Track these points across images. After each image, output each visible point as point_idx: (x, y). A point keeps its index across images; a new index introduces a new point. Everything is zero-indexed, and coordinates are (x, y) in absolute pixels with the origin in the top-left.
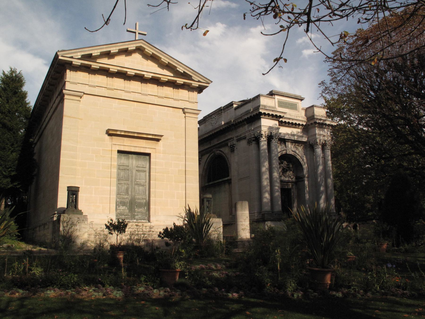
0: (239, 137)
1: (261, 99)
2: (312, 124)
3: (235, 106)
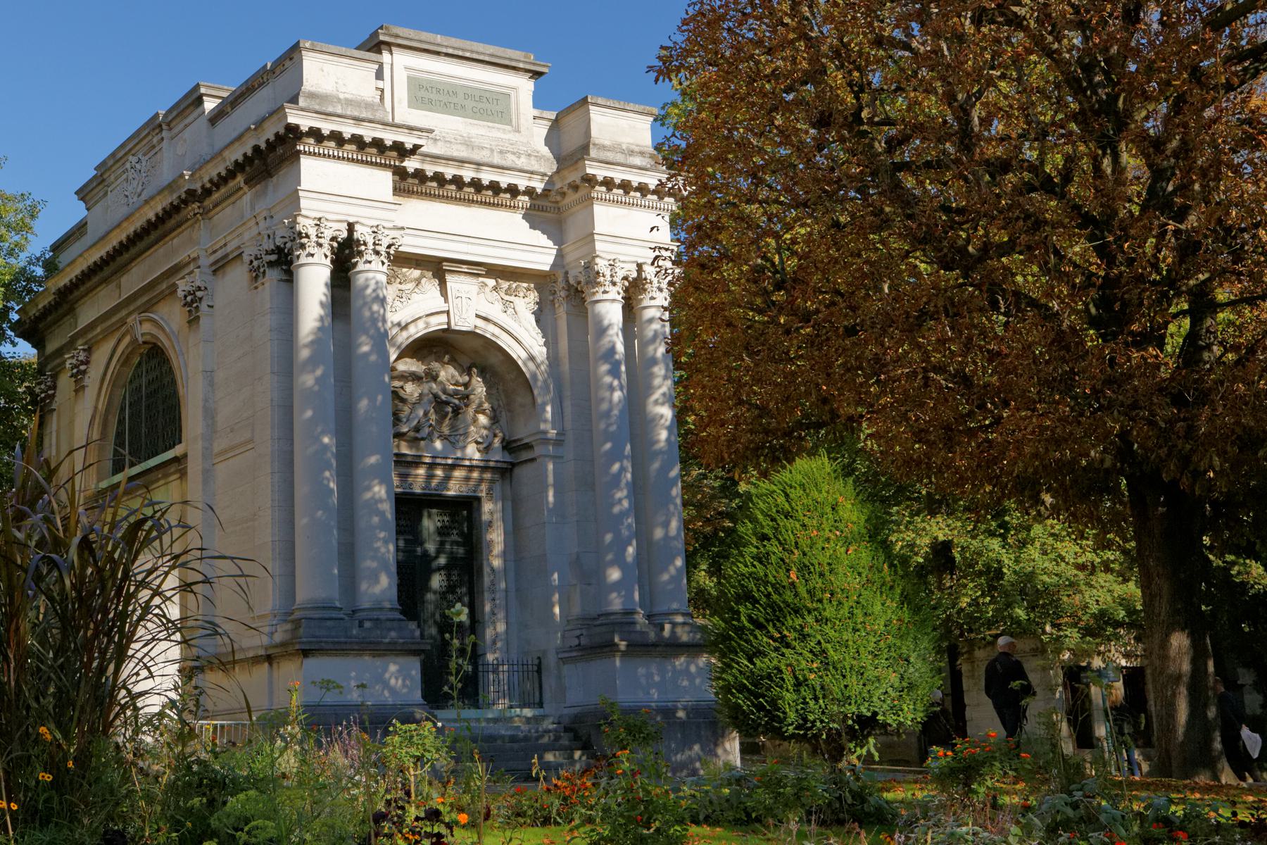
0: (219, 255)
1: (305, 63)
2: (575, 188)
3: (210, 105)
